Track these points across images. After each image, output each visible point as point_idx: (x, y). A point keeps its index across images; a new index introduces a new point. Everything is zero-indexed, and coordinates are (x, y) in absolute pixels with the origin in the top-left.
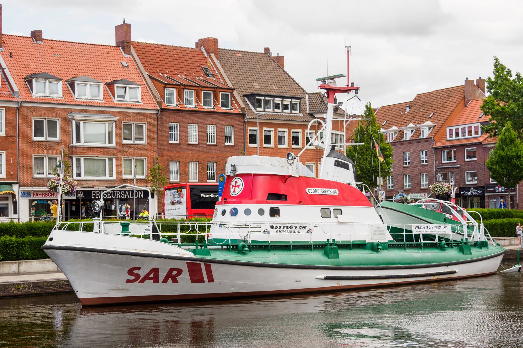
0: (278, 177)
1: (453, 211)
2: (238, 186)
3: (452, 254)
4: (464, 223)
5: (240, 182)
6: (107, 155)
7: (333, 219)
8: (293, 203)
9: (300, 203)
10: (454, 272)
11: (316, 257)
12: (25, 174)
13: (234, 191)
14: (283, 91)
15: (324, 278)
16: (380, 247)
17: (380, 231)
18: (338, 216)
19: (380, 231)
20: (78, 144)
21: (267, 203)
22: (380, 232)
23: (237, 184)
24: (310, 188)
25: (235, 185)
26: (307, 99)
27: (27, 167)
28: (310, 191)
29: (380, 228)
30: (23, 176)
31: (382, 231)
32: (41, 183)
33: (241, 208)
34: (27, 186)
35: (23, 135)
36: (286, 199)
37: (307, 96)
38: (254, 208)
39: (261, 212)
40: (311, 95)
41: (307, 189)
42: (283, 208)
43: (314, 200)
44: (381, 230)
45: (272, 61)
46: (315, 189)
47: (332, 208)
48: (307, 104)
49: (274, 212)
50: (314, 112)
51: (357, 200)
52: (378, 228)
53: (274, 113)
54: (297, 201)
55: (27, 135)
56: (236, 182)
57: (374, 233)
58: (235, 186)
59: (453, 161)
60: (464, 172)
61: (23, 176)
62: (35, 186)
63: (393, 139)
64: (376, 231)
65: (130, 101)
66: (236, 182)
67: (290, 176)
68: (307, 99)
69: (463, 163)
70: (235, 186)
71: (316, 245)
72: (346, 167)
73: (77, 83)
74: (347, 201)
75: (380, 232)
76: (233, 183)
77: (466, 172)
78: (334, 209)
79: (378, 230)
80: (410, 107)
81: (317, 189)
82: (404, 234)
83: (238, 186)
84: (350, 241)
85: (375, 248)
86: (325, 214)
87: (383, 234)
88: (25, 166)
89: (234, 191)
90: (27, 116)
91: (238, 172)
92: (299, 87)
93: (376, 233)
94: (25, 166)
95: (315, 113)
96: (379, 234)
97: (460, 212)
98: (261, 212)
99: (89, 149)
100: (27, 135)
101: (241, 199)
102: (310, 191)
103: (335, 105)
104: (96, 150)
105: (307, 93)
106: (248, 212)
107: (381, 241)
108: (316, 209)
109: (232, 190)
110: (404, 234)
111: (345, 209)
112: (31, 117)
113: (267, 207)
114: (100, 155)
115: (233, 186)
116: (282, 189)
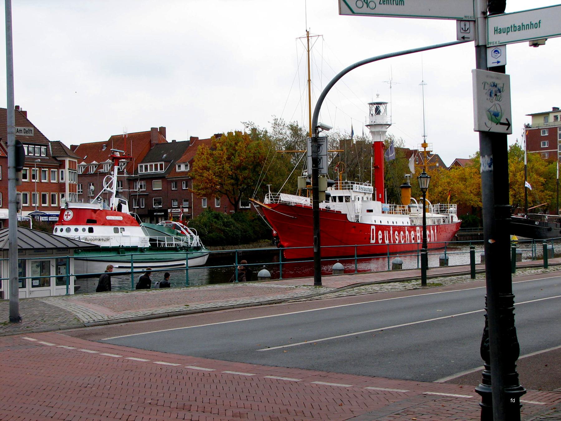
0: (91, 210)
1: (182, 229)
2: (70, 215)
3: (182, 255)
4: (189, 235)
5: (71, 213)
7: (120, 234)
9: (103, 225)
13: (67, 217)
14: (33, 140)
15: (118, 267)
16: (145, 250)
18: (123, 232)
21: (87, 225)
22: (145, 241)
23: (69, 214)
25: (67, 214)
26: (50, 146)
28: (109, 218)
31: (146, 241)
33: (73, 227)
36: (96, 223)
37: (50, 144)
38: (80, 228)
39: (84, 230)
40: (54, 143)
41: (107, 217)
42: (96, 228)
43: (111, 223)
45: (22, 116)
46: (110, 216)
47: (119, 227)
48: (51, 150)
49: (91, 230)
50: (57, 155)
51: (132, 223)
53: (29, 157)
54: (102, 224)
56: (68, 213)
57: (142, 242)
58: (68, 215)
59: (143, 190)
60: (151, 198)
63: (94, 171)
66: (68, 213)
67: (99, 210)
68: (50, 146)
69: (151, 191)
70: (68, 215)
74: (127, 223)
75: (145, 241)
76: (66, 213)
77: (153, 198)
78: (121, 228)
80: (106, 146)
81: (112, 217)
82: (157, 242)
83: (70, 215)
84: (130, 246)
85: (142, 250)
86: (116, 231)
89: (67, 217)
91: (70, 207)
92: (43, 137)
95: (58, 157)
96: (145, 242)
97: (186, 229)
98: (84, 230)
101: (72, 222)
102: (109, 218)
103: (118, 167)
105: (49, 141)
106: (76, 230)
107: (145, 246)
108: (112, 228)
109: (65, 217)
110: (157, 242)
111: (126, 228)
113: (87, 227)
115: (66, 215)
116: (94, 216)
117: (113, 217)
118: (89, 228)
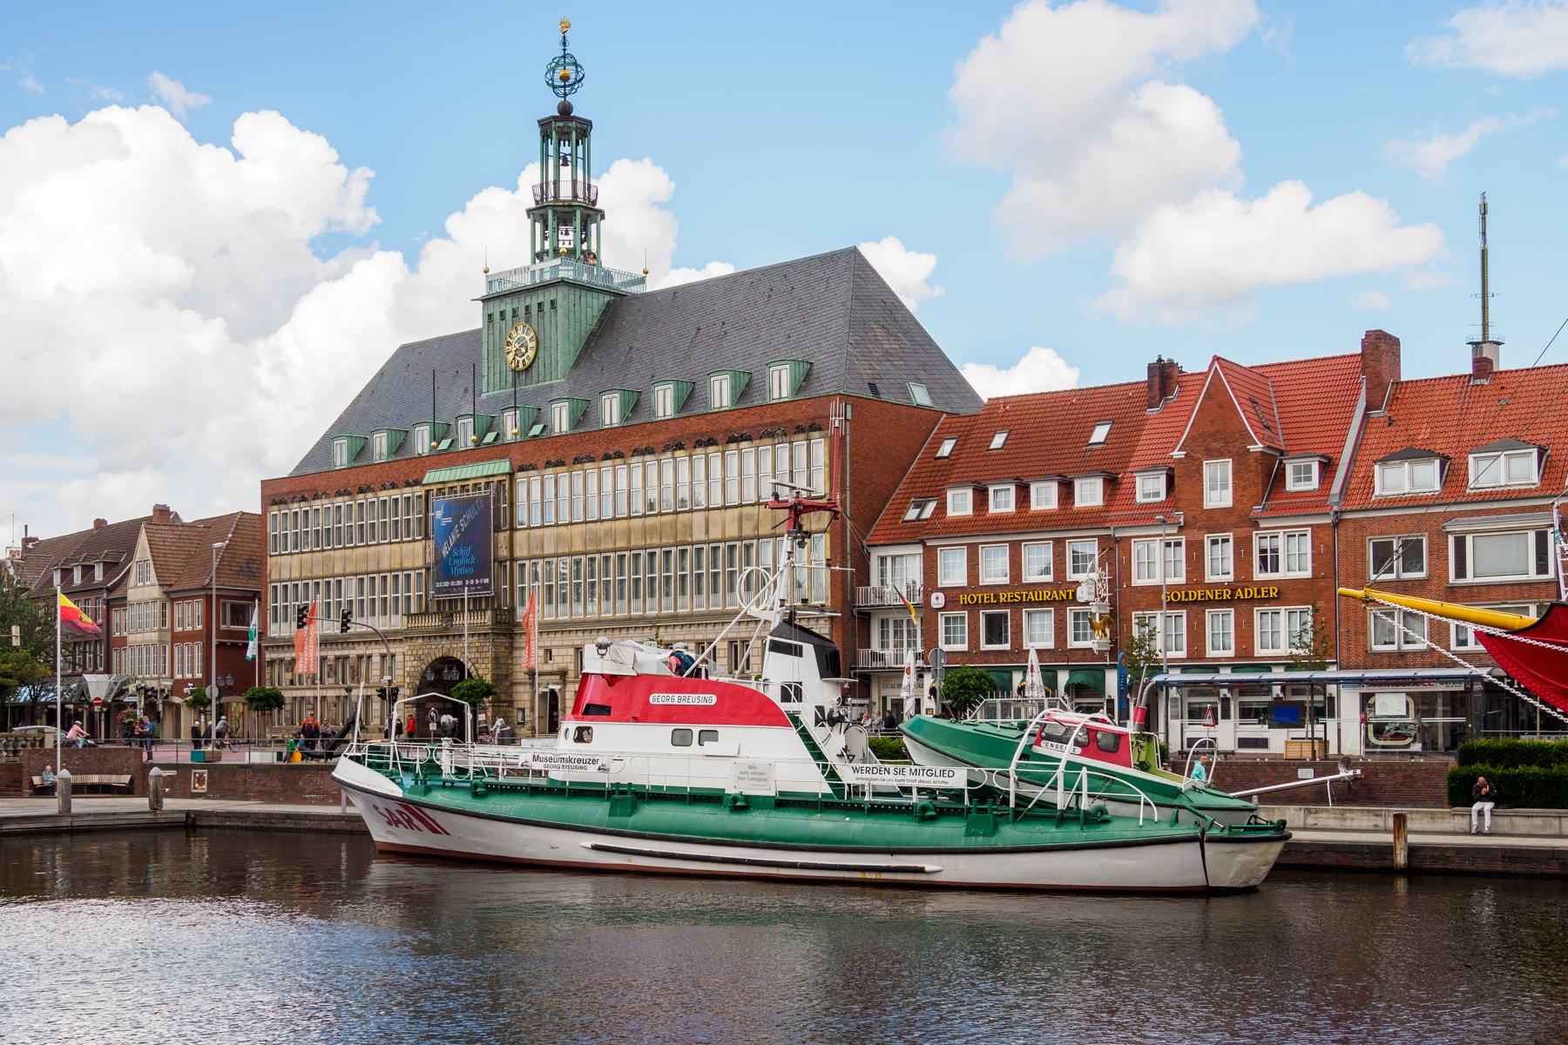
6: (1529, 597)
8: (622, 718)
9: (636, 720)
10: (921, 871)
11: (597, 811)
12: (1352, 646)
17: (756, 773)
19: (756, 773)
20: (1461, 581)
22: (755, 776)
24: (657, 695)
27: (1356, 633)
28: (657, 699)
29: (755, 768)
30: (1348, 649)
32: (1385, 661)
34: (1357, 667)
35: (1347, 574)
44: (757, 771)
46: (666, 695)
47: (696, 729)
52: (750, 767)
55: (1355, 572)
57: (742, 776)
61: (1348, 649)
62: (1373, 667)
64: (747, 773)
65: (1506, 486)
71: (695, 796)
72: (798, 652)
73: (1475, 458)
75: (755, 776)
79: (750, 771)
81: (671, 695)
87: (762, 780)
88: (1352, 631)
90: (1355, 537)
93: (746, 776)
94: (1352, 631)
99: (1483, 590)
100: (1355, 572)
102: (657, 699)
104: (1501, 591)
108: (667, 729)
111: (724, 731)
112: (1363, 537)
114: (1511, 599)
117: (676, 696)
118: (580, 730)
